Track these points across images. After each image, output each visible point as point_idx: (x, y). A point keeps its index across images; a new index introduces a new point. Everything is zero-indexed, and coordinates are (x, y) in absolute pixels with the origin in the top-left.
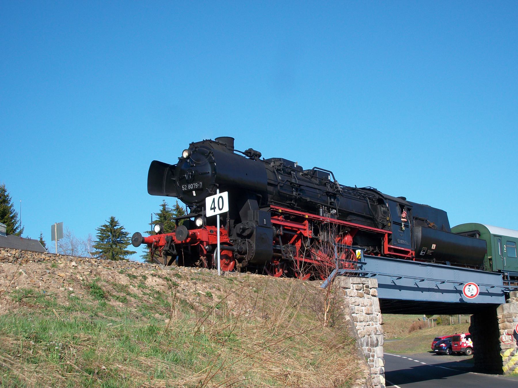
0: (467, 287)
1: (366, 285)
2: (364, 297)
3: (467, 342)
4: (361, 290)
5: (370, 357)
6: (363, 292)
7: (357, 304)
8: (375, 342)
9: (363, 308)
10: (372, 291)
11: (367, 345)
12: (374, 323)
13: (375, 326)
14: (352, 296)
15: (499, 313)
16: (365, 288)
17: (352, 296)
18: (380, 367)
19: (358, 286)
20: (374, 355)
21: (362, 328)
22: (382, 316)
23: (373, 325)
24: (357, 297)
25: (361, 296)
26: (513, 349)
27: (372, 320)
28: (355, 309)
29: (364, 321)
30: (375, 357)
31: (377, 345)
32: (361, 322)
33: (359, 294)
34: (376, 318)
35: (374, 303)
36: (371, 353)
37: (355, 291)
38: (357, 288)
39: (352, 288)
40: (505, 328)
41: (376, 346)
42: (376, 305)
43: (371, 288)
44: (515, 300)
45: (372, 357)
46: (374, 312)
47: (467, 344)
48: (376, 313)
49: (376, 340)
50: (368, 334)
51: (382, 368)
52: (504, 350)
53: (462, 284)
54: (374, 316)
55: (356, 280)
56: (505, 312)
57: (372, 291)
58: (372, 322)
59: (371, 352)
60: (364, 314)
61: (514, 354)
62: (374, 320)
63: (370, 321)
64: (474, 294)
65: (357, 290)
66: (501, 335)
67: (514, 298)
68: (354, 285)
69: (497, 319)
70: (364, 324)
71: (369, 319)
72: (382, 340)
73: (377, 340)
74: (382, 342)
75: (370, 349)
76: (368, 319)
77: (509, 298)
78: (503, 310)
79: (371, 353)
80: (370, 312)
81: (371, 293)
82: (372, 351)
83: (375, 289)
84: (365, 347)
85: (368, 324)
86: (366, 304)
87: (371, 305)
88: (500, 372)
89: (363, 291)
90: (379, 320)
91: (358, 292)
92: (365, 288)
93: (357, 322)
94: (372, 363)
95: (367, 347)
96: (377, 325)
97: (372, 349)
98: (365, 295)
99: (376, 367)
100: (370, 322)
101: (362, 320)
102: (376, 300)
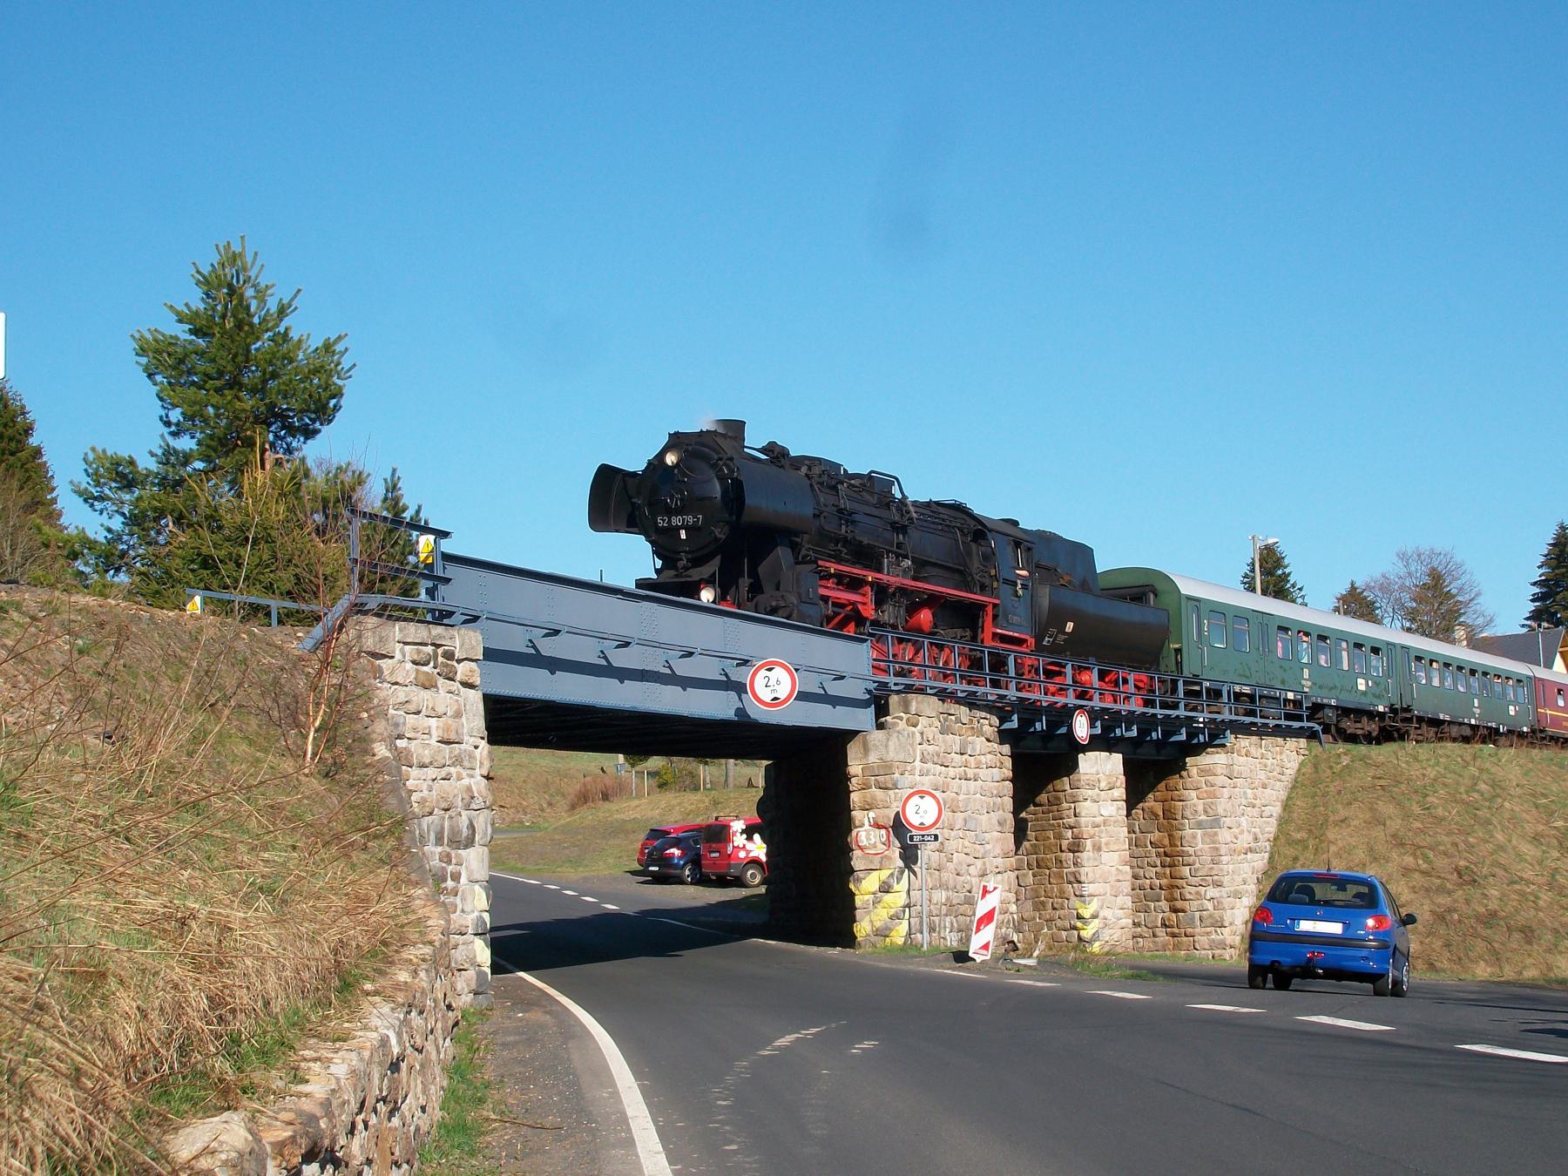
0: (763, 673)
1: (446, 648)
2: (436, 686)
3: (749, 846)
4: (429, 664)
5: (446, 881)
6: (433, 670)
7: (412, 707)
8: (465, 832)
9: (433, 722)
10: (462, 670)
11: (439, 841)
12: (464, 773)
13: (466, 781)
14: (396, 683)
15: (855, 759)
16: (440, 659)
17: (396, 683)
18: (476, 914)
19: (419, 652)
20: (460, 874)
21: (425, 787)
22: (489, 752)
23: (459, 778)
24: (414, 688)
25: (427, 685)
26: (890, 872)
27: (458, 761)
28: (404, 724)
29: (431, 763)
30: (463, 880)
31: (470, 843)
32: (423, 766)
33: (421, 678)
34: (470, 757)
35: (468, 707)
36: (450, 868)
37: (409, 666)
38: (415, 657)
39: (398, 656)
40: (867, 807)
41: (466, 847)
42: (474, 715)
43: (459, 661)
44: (904, 720)
45: (452, 880)
46: (466, 738)
47: (748, 852)
48: (473, 739)
49: (467, 828)
50: (444, 805)
51: (481, 916)
52: (861, 875)
53: (745, 662)
54: (465, 751)
55: (415, 631)
56: (873, 758)
57: (462, 670)
58: (459, 768)
59: (449, 862)
60: (433, 742)
61: (890, 887)
62: (466, 764)
63: (453, 765)
64: (783, 696)
65: (414, 662)
66: (856, 827)
67: (902, 714)
68: (407, 648)
69: (847, 778)
70: (431, 772)
71: (450, 758)
72: (486, 828)
73: (472, 827)
74: (485, 834)
75: (449, 855)
76: (444, 758)
77: (887, 714)
78: (866, 750)
79: (450, 868)
80: (453, 737)
81: (459, 677)
82: (454, 861)
83: (473, 665)
84: (433, 849)
85: (443, 774)
86: (440, 710)
87: (458, 715)
88: (846, 938)
89: (435, 668)
90: (481, 763)
91: (417, 671)
92: (440, 659)
93: (411, 767)
94: (452, 899)
95: (439, 849)
96: (472, 779)
97: (453, 853)
98: (441, 681)
99: (463, 911)
100: (452, 770)
101: (427, 761)
102: (475, 700)
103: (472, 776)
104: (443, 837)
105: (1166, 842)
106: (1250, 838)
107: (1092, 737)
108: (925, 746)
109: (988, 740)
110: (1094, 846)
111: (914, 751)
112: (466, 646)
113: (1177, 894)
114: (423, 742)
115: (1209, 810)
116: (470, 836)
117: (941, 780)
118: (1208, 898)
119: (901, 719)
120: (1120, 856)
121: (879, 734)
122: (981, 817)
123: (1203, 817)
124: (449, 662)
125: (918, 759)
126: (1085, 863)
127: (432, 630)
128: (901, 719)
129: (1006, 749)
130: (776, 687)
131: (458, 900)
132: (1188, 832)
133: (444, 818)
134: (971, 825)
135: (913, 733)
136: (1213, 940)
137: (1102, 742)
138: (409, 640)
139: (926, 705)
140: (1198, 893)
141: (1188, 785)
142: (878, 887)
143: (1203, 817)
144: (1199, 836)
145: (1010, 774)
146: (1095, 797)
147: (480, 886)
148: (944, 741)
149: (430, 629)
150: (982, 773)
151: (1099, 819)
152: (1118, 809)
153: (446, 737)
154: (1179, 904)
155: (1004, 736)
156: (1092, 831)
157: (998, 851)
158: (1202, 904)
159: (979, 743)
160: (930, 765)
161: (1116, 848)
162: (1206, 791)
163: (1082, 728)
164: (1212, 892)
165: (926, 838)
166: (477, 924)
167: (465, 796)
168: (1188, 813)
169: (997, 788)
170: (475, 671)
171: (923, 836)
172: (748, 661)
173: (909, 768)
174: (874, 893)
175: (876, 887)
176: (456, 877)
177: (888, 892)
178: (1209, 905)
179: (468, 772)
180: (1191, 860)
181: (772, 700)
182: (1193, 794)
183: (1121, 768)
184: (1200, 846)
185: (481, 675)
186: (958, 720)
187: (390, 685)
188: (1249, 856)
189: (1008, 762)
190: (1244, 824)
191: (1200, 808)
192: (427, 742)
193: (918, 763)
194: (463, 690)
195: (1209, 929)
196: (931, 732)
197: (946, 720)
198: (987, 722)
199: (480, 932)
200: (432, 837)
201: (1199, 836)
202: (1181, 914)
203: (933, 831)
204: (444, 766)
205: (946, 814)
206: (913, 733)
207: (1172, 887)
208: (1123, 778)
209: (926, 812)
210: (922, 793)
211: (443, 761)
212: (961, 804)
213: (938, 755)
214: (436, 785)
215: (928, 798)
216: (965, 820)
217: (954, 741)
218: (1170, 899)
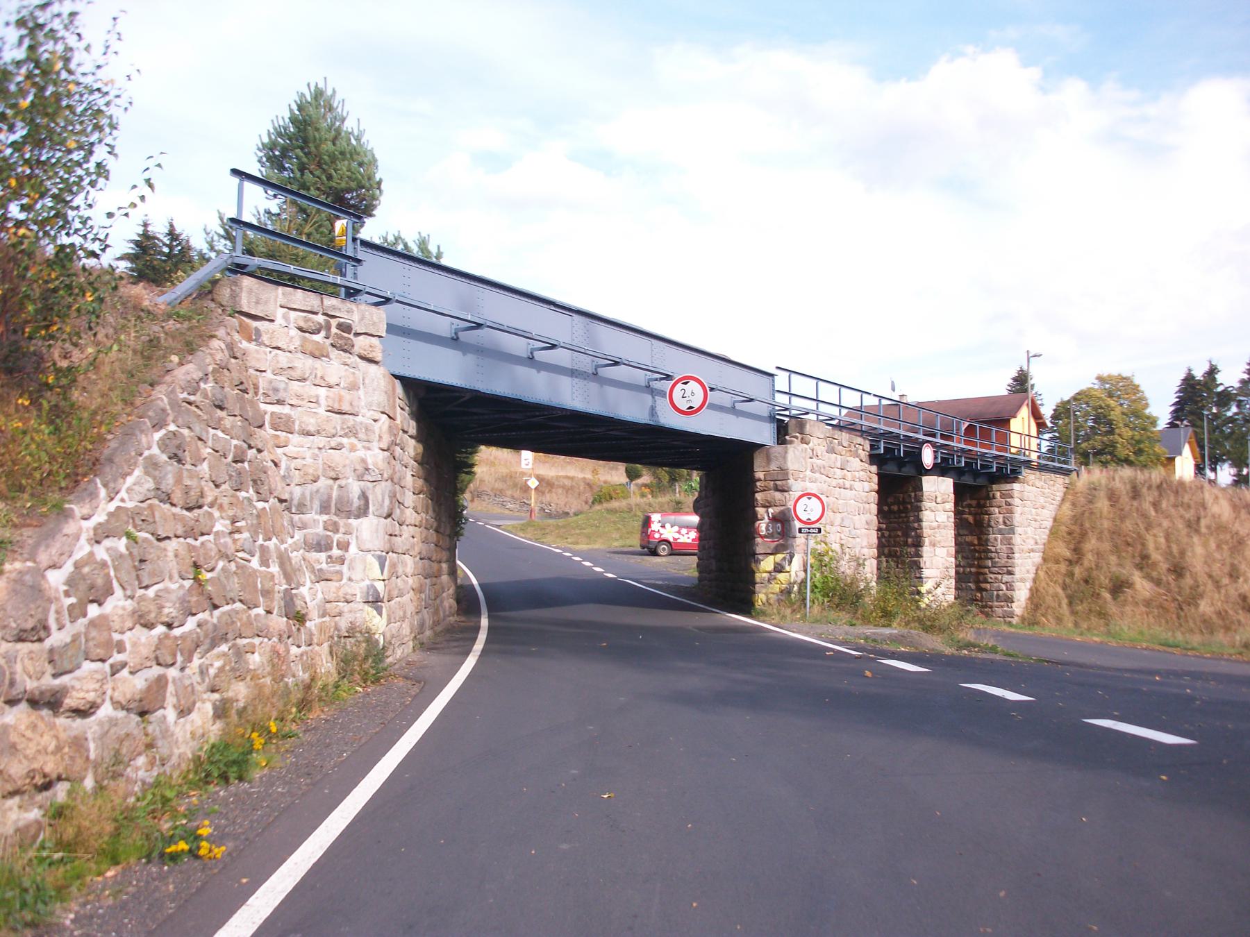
0: (680, 386)
1: (342, 320)
2: (327, 356)
3: (662, 531)
4: (319, 333)
5: (331, 549)
6: (326, 340)
7: (296, 374)
8: (356, 503)
9: (322, 392)
10: (361, 343)
11: (325, 509)
12: (359, 445)
13: (361, 453)
14: (278, 348)
15: (760, 466)
16: (334, 330)
17: (278, 348)
18: (368, 582)
19: (306, 320)
20: (348, 544)
21: (308, 454)
22: (390, 427)
23: (353, 449)
24: (300, 355)
25: (317, 354)
26: (783, 556)
27: (352, 432)
28: (285, 390)
29: (318, 432)
30: (353, 549)
31: (363, 512)
32: (309, 434)
33: (309, 347)
34: (367, 429)
35: (367, 381)
36: (336, 537)
37: (294, 332)
38: (302, 324)
39: (280, 320)
40: (767, 504)
41: (358, 517)
42: (374, 390)
43: (357, 335)
44: (799, 439)
45: (339, 548)
46: (364, 411)
47: (661, 534)
48: (372, 412)
49: (359, 498)
50: (333, 474)
51: (373, 586)
52: (760, 557)
53: (668, 377)
54: (361, 423)
55: (300, 298)
56: (773, 466)
57: (361, 343)
58: (353, 440)
59: (336, 531)
60: (322, 411)
61: (783, 567)
62: (362, 436)
63: (346, 435)
64: (696, 406)
65: (301, 329)
66: (758, 520)
67: (797, 434)
68: (293, 314)
69: (754, 481)
70: (319, 441)
71: (342, 429)
72: (383, 501)
73: (364, 496)
74: (382, 506)
75: (335, 524)
76: (335, 428)
77: (787, 434)
78: (769, 460)
79: (336, 537)
80: (345, 408)
81: (356, 349)
82: (342, 530)
83: (375, 341)
84: (317, 517)
85: (333, 444)
86: (332, 381)
87: (353, 387)
88: (745, 605)
89: (327, 338)
90: (380, 437)
91: (305, 339)
92: (334, 330)
93: (292, 433)
94: (338, 567)
95: (325, 517)
96: (369, 451)
97: (341, 522)
98: (334, 353)
99: (350, 579)
100: (345, 441)
101: (312, 429)
102: (377, 376)
103: (369, 449)
104: (330, 506)
105: (976, 542)
106: (1032, 542)
107: (935, 465)
108: (814, 460)
109: (862, 461)
110: (931, 543)
111: (806, 463)
112: (366, 321)
113: (981, 578)
114: (309, 410)
115: (1007, 522)
116: (362, 507)
117: (825, 486)
118: (1004, 581)
119: (797, 437)
120: (948, 551)
121: (780, 448)
122: (854, 518)
123: (1003, 527)
124: (346, 335)
125: (809, 469)
126: (924, 555)
127: (324, 300)
128: (797, 437)
129: (874, 468)
130: (691, 398)
131: (345, 568)
132: (992, 537)
133: (331, 488)
134: (846, 523)
135: (806, 449)
136: (1006, 611)
137: (941, 469)
138: (295, 307)
139: (816, 428)
140: (996, 578)
141: (994, 504)
142: (773, 567)
143: (1003, 527)
144: (999, 540)
145: (876, 487)
146: (933, 509)
147: (373, 555)
148: (829, 458)
149: (322, 299)
150: (857, 485)
151: (935, 524)
152: (948, 517)
153: (336, 407)
154: (983, 585)
155: (874, 459)
156: (930, 532)
157: (865, 543)
158: (999, 586)
159: (855, 463)
160: (817, 475)
161: (945, 545)
162: (1006, 509)
163: (928, 457)
164: (1006, 578)
165: (811, 531)
166: (368, 593)
167: (358, 467)
168: (992, 523)
169: (867, 497)
170: (375, 347)
171: (809, 529)
172: (670, 376)
173: (801, 476)
174: (770, 572)
175: (770, 567)
176: (344, 546)
177: (781, 572)
178: (1004, 587)
179: (365, 444)
180: (993, 555)
181: (688, 409)
182: (997, 510)
183: (952, 489)
184: (999, 546)
185: (383, 351)
186: (840, 444)
187: (269, 349)
188: (1032, 554)
189: (875, 479)
190: (1029, 532)
191: (1001, 520)
192: (314, 410)
193: (808, 473)
194: (363, 364)
195: (1002, 604)
196: (821, 449)
197: (831, 443)
198: (861, 447)
199: (370, 600)
200: (316, 505)
201: (999, 540)
202: (984, 593)
203: (817, 525)
204: (334, 436)
205: (828, 513)
206: (806, 449)
207: (978, 574)
208: (952, 496)
209: (812, 510)
210: (809, 495)
211: (333, 431)
212: (840, 507)
213: (824, 468)
214: (323, 455)
215: (814, 499)
216: (843, 520)
217: (836, 459)
218: (977, 582)
